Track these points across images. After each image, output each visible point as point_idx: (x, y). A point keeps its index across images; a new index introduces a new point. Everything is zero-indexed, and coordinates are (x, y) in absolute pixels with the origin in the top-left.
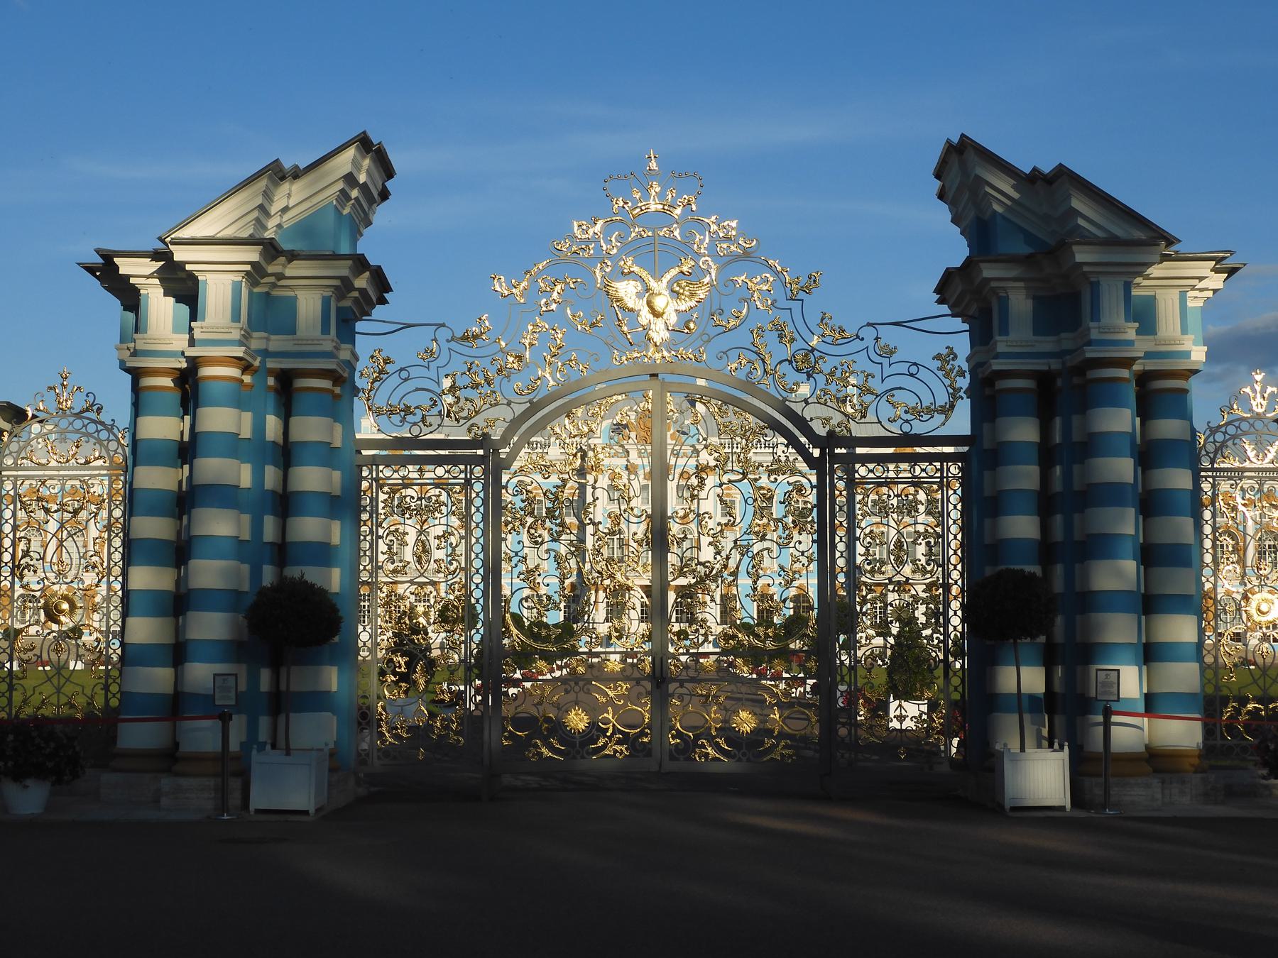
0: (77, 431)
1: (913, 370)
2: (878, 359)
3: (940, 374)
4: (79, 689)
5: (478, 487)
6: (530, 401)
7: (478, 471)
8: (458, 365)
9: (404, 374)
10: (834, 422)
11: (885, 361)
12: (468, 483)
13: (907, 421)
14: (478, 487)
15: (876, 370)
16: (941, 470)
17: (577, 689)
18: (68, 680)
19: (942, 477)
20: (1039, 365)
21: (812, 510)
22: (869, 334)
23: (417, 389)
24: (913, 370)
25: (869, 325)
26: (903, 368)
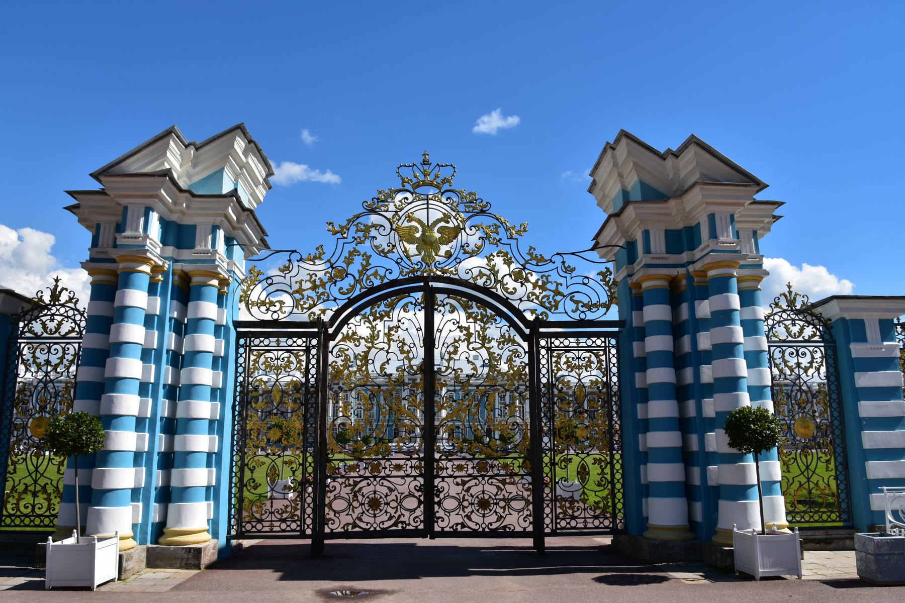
0: (61, 315)
1: (586, 281)
2: (565, 275)
3: (602, 283)
4: (49, 482)
5: (314, 352)
6: (348, 298)
7: (314, 342)
8: (303, 275)
9: (269, 281)
10: (538, 312)
11: (568, 276)
12: (307, 351)
13: (583, 312)
14: (314, 352)
15: (562, 280)
16: (605, 342)
17: (375, 483)
18: (42, 475)
19: (605, 347)
20: (673, 272)
21: (524, 368)
22: (558, 259)
23: (277, 290)
24: (586, 281)
25: (558, 254)
26: (580, 280)
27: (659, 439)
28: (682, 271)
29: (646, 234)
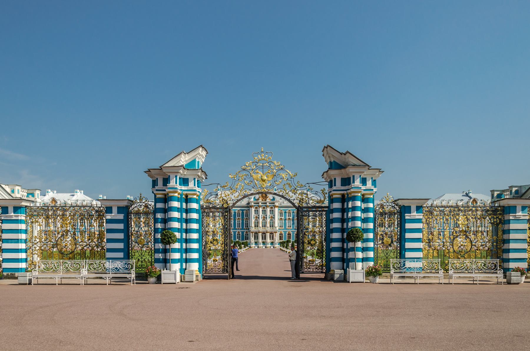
20: (342, 192)
22: (307, 185)
27: (334, 245)
28: (345, 192)
29: (335, 179)
